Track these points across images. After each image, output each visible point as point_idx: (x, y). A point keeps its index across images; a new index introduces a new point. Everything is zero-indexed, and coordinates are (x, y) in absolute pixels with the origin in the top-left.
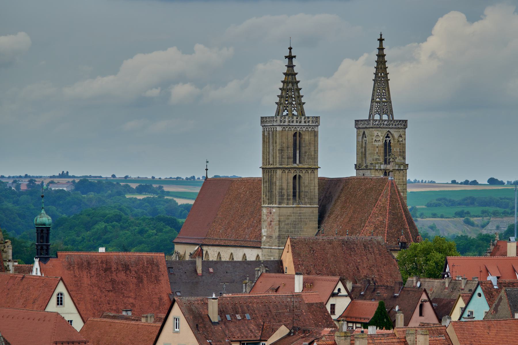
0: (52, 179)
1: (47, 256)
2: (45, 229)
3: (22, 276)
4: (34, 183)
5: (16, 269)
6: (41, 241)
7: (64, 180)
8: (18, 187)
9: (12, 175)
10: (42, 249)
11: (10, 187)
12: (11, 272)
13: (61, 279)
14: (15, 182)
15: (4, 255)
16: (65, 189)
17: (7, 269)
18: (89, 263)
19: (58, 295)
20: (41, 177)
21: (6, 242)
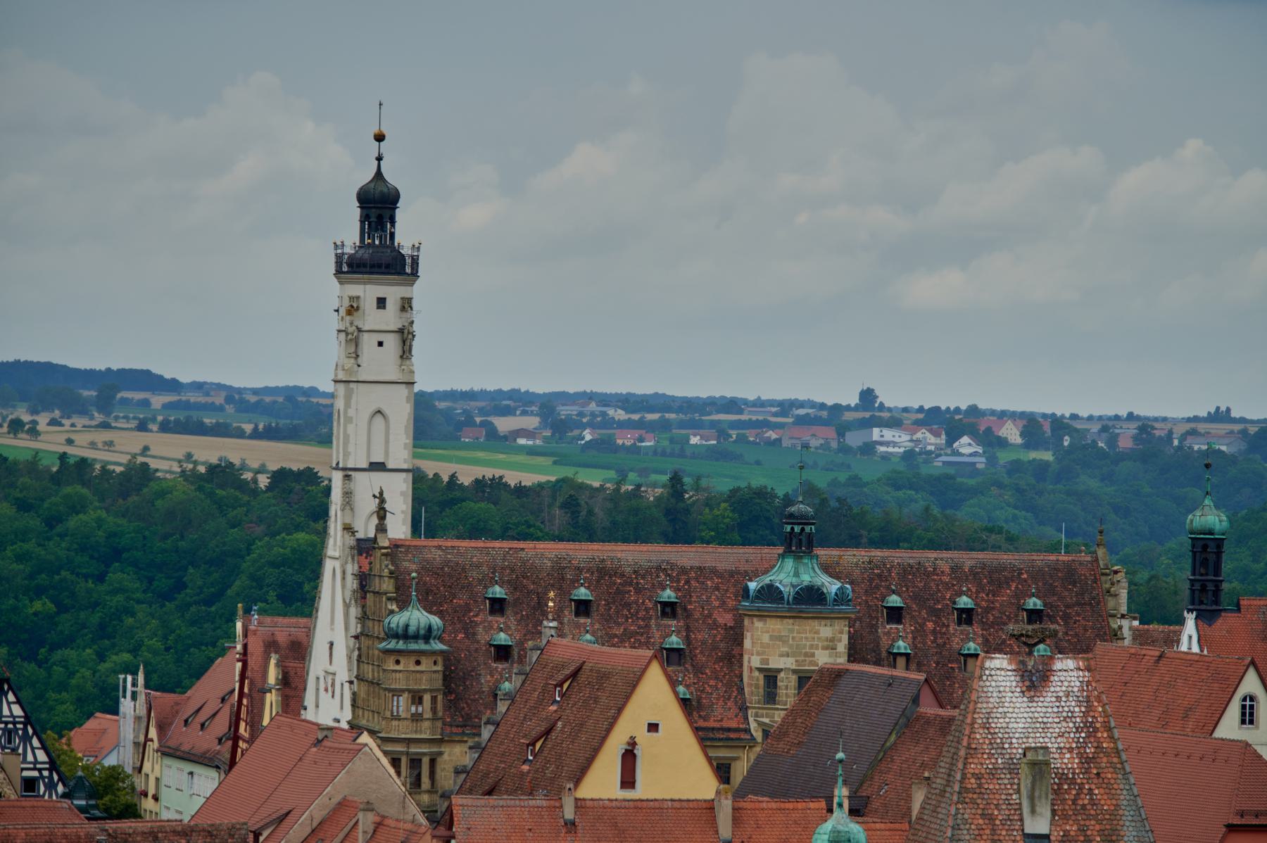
0: (1193, 425)
1: (1214, 607)
2: (1212, 544)
3: (1157, 654)
4: (1149, 434)
5: (1138, 636)
6: (1203, 571)
7: (1224, 428)
8: (1113, 441)
9: (1096, 413)
10: (1204, 589)
11: (1094, 442)
12: (1127, 642)
13: (1253, 663)
14: (1105, 429)
15: (1111, 603)
16: (1224, 448)
17: (1116, 635)
19: (1244, 699)
20: (1165, 419)
21: (1116, 572)
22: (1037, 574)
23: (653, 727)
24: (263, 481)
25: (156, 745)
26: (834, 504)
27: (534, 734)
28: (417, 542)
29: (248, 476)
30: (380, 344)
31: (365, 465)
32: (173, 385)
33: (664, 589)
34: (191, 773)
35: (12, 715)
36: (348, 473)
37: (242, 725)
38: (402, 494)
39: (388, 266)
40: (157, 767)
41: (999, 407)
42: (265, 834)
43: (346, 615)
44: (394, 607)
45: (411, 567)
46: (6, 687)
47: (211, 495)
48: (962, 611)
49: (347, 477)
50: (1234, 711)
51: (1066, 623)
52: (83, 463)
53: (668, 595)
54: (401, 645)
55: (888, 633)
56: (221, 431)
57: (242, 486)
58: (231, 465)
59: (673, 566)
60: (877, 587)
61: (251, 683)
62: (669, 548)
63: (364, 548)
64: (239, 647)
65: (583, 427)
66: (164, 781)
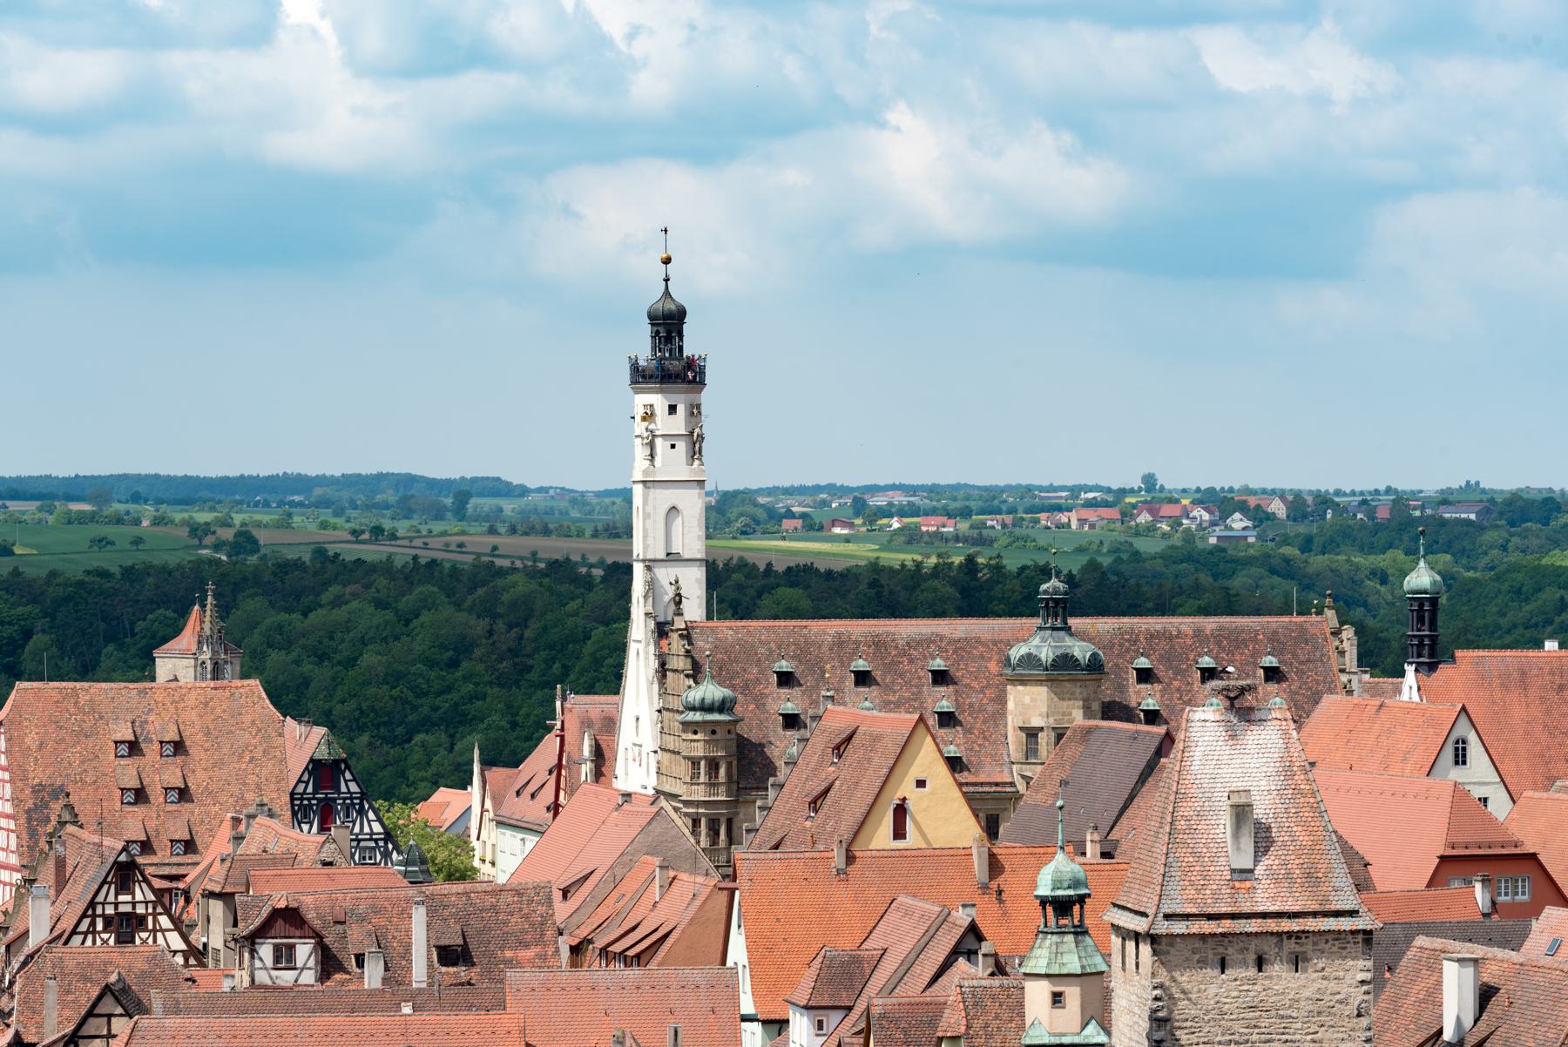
8: (1371, 513)
9: (1358, 489)
10: (1421, 645)
13: (1464, 709)
18: (1523, 673)
22: (1273, 637)
23: (921, 783)
24: (598, 573)
25: (491, 815)
26: (1115, 578)
27: (815, 793)
28: (710, 624)
29: (584, 570)
30: (673, 446)
31: (662, 556)
32: (523, 491)
33: (934, 658)
36: (649, 565)
37: (562, 793)
38: (697, 580)
39: (677, 376)
40: (493, 835)
41: (1269, 487)
43: (650, 690)
44: (691, 682)
45: (703, 645)
47: (550, 589)
48: (1203, 670)
49: (649, 568)
50: (1449, 753)
51: (1300, 678)
52: (433, 563)
53: (939, 664)
54: (698, 716)
55: (1138, 693)
57: (576, 579)
58: (568, 560)
59: (942, 638)
60: (1128, 650)
62: (936, 622)
63: (662, 630)
64: (559, 724)
65: (891, 516)
66: (498, 848)
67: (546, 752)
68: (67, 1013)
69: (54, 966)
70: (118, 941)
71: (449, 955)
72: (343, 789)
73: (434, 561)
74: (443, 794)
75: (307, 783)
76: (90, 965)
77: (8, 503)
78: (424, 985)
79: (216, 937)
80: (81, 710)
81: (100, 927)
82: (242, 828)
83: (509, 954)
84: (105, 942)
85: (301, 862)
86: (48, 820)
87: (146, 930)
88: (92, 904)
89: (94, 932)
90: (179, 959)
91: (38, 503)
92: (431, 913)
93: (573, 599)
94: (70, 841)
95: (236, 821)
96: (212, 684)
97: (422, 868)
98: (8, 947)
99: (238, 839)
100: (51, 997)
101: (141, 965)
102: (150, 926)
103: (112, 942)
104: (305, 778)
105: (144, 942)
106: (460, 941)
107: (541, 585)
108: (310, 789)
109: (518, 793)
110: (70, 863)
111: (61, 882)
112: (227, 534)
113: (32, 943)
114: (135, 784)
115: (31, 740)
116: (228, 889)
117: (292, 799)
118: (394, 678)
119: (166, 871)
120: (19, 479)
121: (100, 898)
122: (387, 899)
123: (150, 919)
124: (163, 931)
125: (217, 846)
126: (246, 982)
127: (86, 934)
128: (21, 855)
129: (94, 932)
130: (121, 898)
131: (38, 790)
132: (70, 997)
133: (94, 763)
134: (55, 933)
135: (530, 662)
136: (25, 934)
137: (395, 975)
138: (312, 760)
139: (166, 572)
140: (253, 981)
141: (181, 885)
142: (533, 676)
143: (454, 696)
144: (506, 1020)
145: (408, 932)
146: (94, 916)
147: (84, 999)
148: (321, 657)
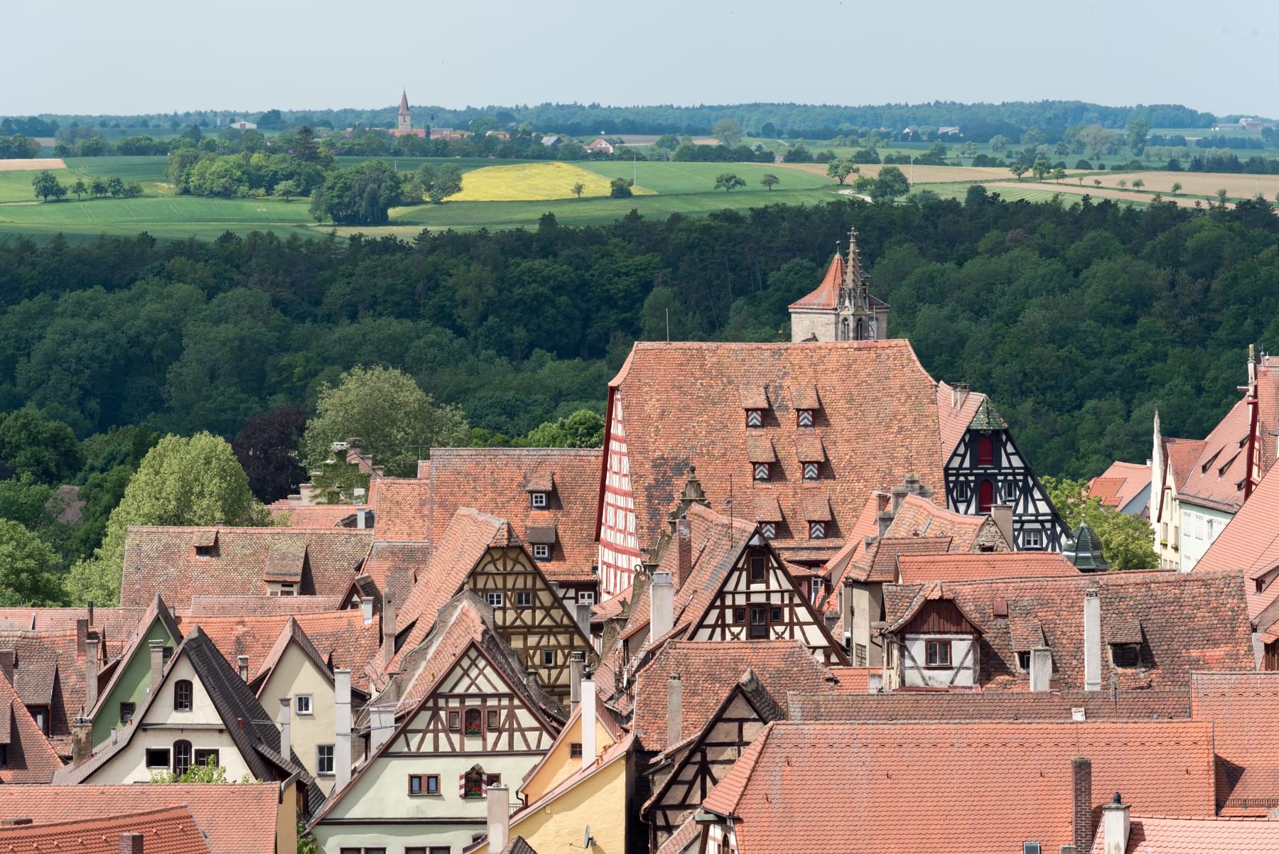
25: (1174, 492)
32: (1210, 120)
34: (1210, 521)
35: (1011, 467)
37: (1255, 469)
40: (1176, 515)
42: (1268, 581)
46: (1004, 438)
47: (1242, 235)
52: (1107, 203)
56: (1257, 167)
58: (1261, 201)
61: (1263, 426)
64: (1251, 389)
66: (1182, 531)
67: (1237, 421)
68: (694, 717)
69: (678, 664)
70: (750, 636)
71: (1127, 654)
72: (1005, 463)
73: (1107, 202)
74: (1118, 470)
75: (963, 457)
76: (719, 662)
77: (624, 137)
78: (1098, 688)
79: (861, 632)
80: (707, 373)
81: (729, 617)
82: (890, 507)
83: (1195, 653)
84: (735, 636)
85: (954, 545)
86: (670, 499)
87: (782, 623)
88: (721, 594)
89: (724, 626)
90: (820, 657)
91: (658, 138)
92: (1106, 605)
93: (1267, 245)
94: (696, 523)
95: (884, 500)
96: (855, 344)
97: (1094, 555)
98: (626, 642)
99: (886, 520)
100: (675, 699)
101: (776, 663)
102: (787, 619)
103: (743, 636)
104: (961, 450)
105: (780, 636)
106: (1139, 639)
107: (1231, 229)
108: (967, 464)
109: (1205, 469)
110: (696, 547)
111: (686, 569)
112: (871, 172)
113: (653, 639)
114: (770, 457)
115: (652, 407)
116: (875, 578)
117: (947, 475)
118: (1060, 336)
119: (804, 556)
120: (636, 111)
121: (730, 587)
122: (1057, 590)
123: (786, 610)
124: (801, 624)
125: (861, 528)
126: (896, 683)
127: (714, 627)
128: (641, 538)
129: (724, 626)
130: (754, 587)
131: (659, 463)
132: (696, 700)
133: (723, 434)
134: (679, 627)
135: (1218, 317)
136: (645, 627)
137: (1064, 676)
138: (969, 430)
139: (800, 212)
140: (903, 682)
141: (821, 573)
142: (1221, 334)
143: (1130, 357)
144: (1192, 730)
145: (1080, 628)
146: (723, 607)
147: (712, 702)
148: (979, 311)
